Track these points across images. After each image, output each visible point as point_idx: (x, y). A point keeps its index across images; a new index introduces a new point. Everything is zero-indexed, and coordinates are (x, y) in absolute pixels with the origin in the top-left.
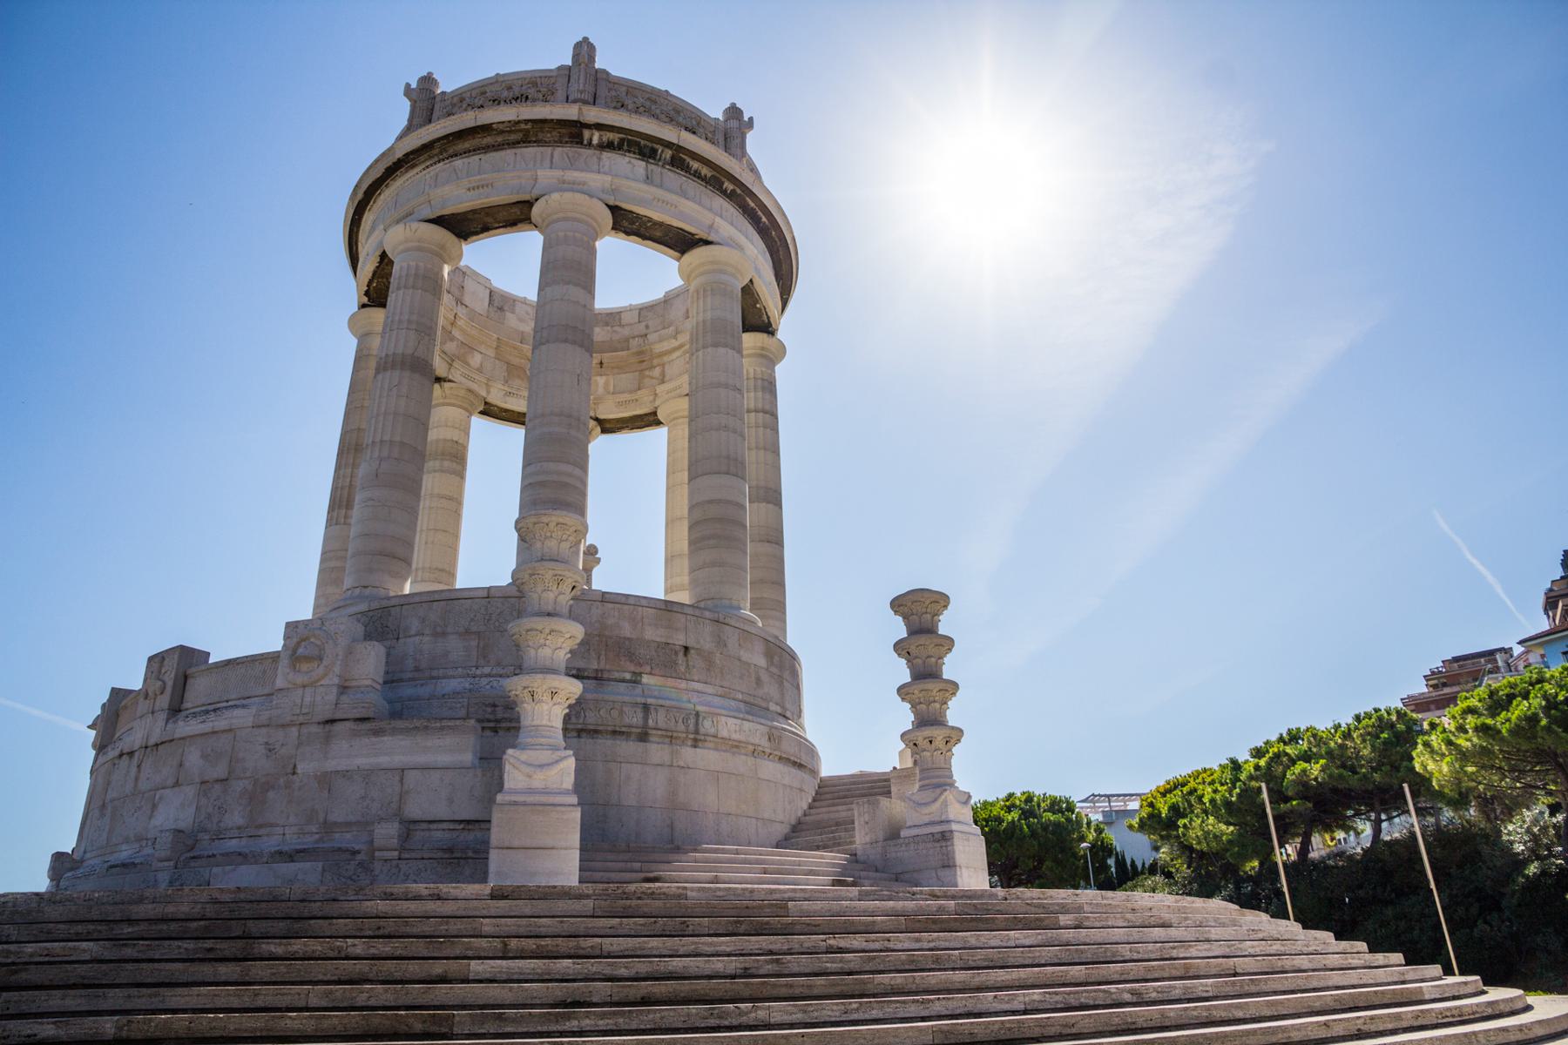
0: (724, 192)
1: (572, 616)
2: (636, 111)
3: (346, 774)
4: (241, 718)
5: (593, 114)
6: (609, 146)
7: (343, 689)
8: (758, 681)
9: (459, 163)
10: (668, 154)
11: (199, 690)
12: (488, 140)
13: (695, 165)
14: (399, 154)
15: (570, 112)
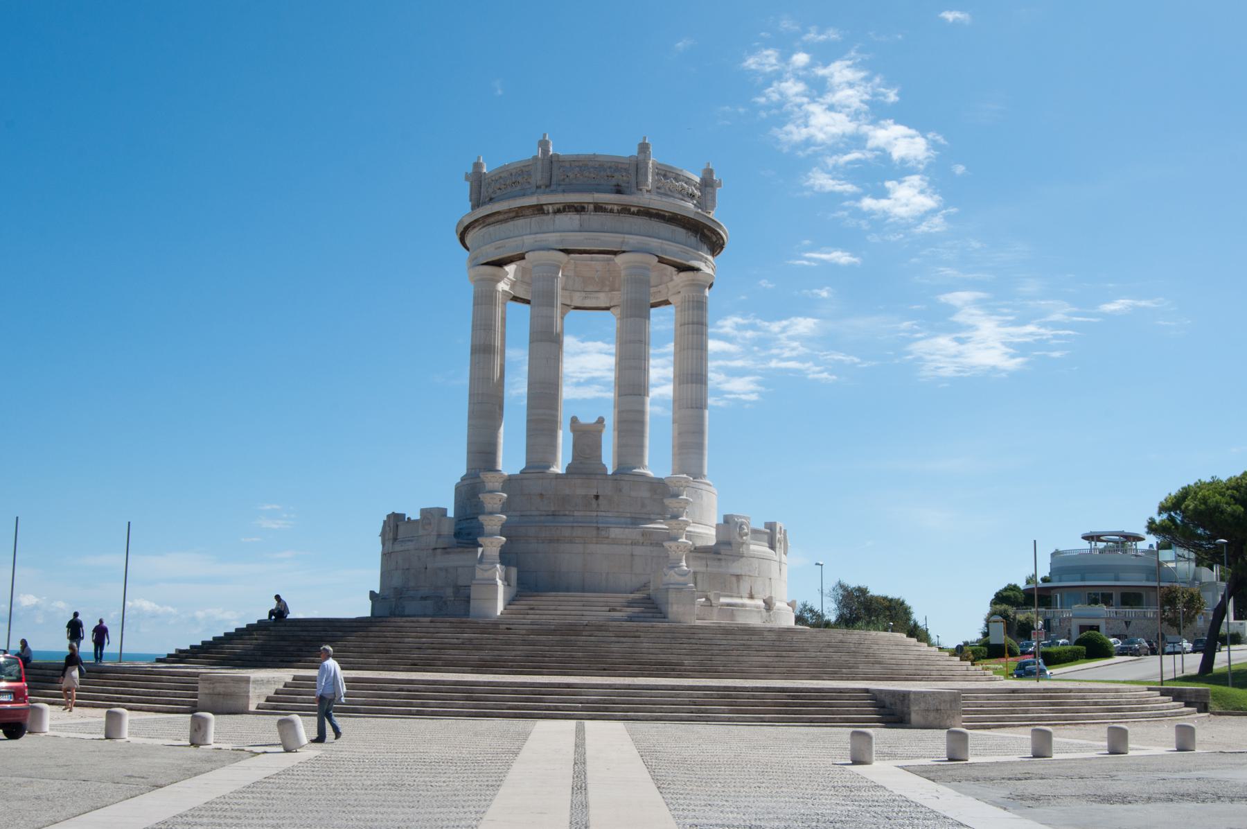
0: (633, 213)
1: (502, 513)
2: (564, 191)
3: (441, 569)
4: (410, 546)
5: (544, 199)
6: (558, 211)
7: (439, 536)
8: (643, 506)
9: (491, 229)
10: (591, 207)
11: (402, 529)
12: (501, 217)
13: (609, 207)
14: (466, 223)
15: (532, 201)
